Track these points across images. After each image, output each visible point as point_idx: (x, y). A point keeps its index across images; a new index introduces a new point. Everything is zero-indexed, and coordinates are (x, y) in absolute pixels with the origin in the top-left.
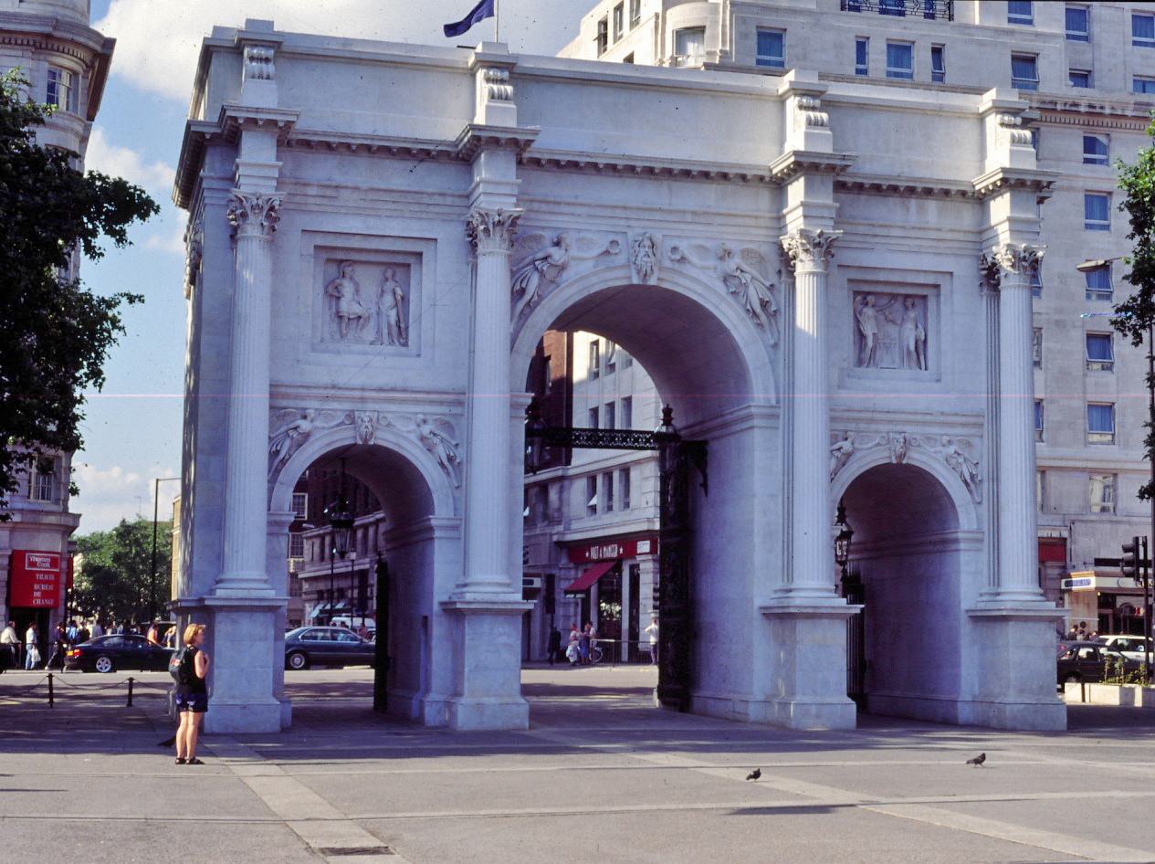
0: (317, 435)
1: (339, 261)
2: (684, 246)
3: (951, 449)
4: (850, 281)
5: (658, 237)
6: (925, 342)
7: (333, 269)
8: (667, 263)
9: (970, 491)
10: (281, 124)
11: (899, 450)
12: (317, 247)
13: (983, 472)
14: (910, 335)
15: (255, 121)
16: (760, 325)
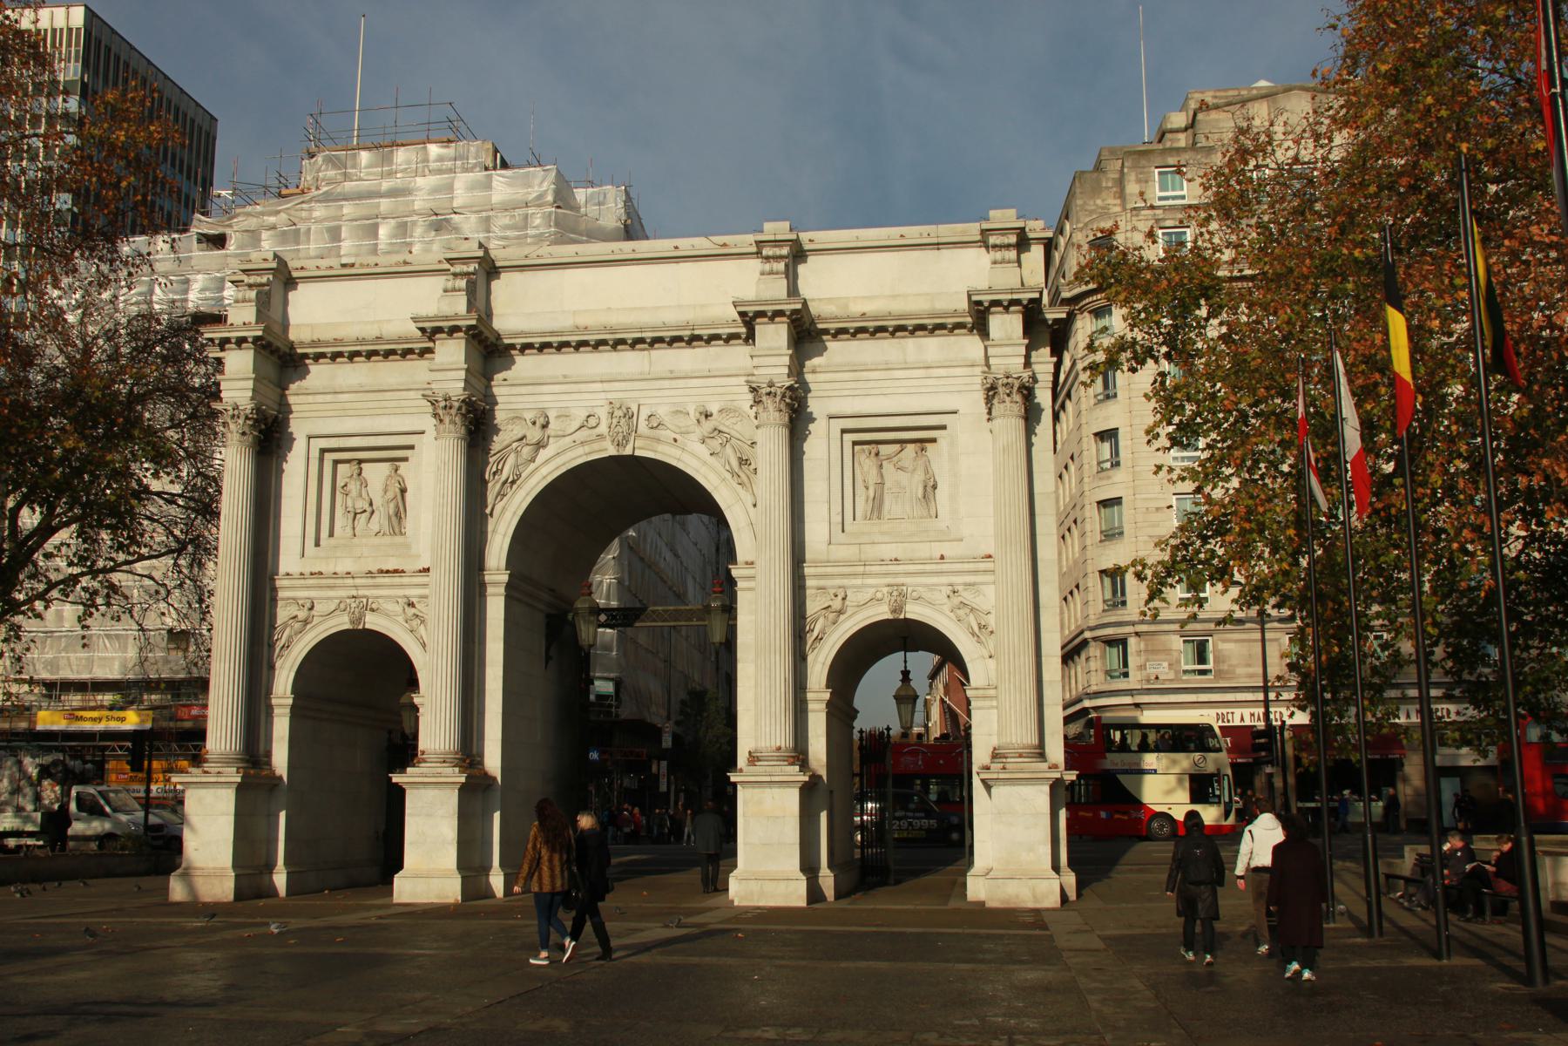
0: (316, 620)
1: (345, 457)
2: (663, 412)
3: (956, 600)
5: (635, 409)
6: (935, 487)
13: (991, 621)
14: (919, 476)
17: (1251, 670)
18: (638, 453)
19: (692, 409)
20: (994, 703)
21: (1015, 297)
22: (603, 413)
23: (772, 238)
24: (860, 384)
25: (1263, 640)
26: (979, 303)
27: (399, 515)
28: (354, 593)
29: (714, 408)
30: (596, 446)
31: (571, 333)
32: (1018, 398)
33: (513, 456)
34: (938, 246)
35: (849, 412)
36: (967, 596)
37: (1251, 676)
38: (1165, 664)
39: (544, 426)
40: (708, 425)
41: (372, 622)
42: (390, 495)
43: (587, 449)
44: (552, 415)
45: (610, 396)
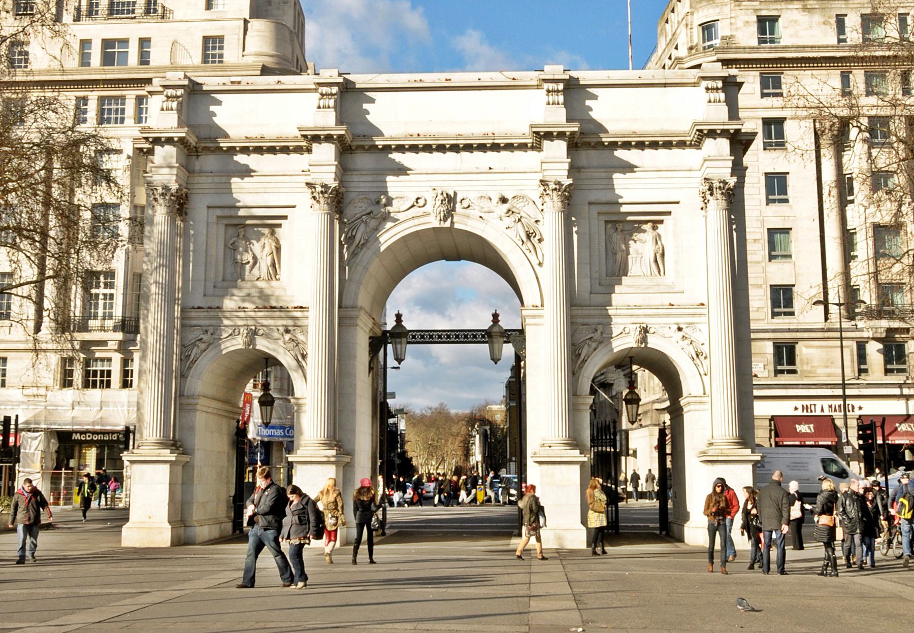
6: (663, 255)
7: (231, 231)
10: (176, 139)
12: (218, 217)
17: (829, 371)
21: (726, 127)
22: (429, 196)
23: (551, 77)
25: (842, 347)
26: (700, 131)
29: (509, 196)
30: (422, 220)
31: (406, 139)
33: (363, 226)
34: (665, 85)
35: (604, 200)
37: (829, 375)
38: (761, 365)
43: (417, 221)
45: (434, 184)
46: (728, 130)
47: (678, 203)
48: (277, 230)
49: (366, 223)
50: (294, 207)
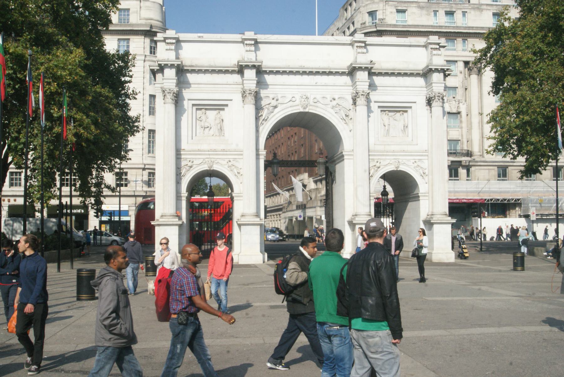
0: (194, 166)
2: (319, 97)
3: (416, 164)
4: (379, 107)
5: (309, 96)
6: (407, 127)
7: (198, 112)
8: (312, 103)
9: (423, 178)
11: (397, 166)
12: (193, 105)
13: (426, 171)
15: (167, 65)
16: (346, 123)
18: (310, 111)
19: (329, 98)
20: (427, 198)
21: (443, 68)
24: (385, 91)
26: (431, 69)
27: (221, 129)
28: (208, 157)
29: (336, 97)
30: (295, 108)
32: (441, 100)
34: (410, 46)
36: (419, 163)
39: (277, 100)
40: (334, 103)
41: (216, 167)
42: (218, 121)
43: (292, 108)
44: (279, 96)
46: (443, 69)
47: (415, 102)
48: (221, 112)
49: (268, 109)
50: (231, 100)
